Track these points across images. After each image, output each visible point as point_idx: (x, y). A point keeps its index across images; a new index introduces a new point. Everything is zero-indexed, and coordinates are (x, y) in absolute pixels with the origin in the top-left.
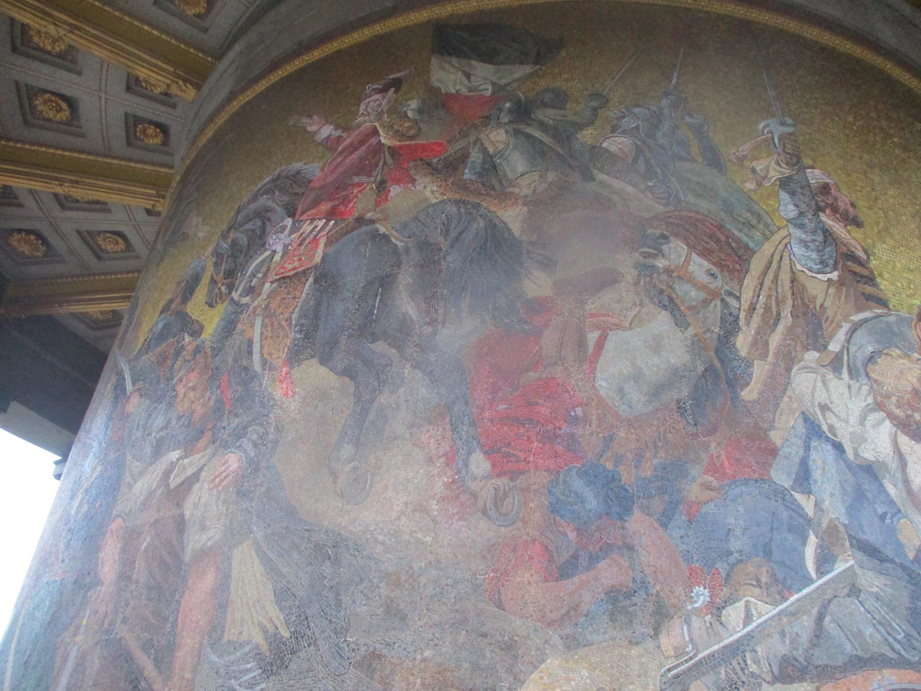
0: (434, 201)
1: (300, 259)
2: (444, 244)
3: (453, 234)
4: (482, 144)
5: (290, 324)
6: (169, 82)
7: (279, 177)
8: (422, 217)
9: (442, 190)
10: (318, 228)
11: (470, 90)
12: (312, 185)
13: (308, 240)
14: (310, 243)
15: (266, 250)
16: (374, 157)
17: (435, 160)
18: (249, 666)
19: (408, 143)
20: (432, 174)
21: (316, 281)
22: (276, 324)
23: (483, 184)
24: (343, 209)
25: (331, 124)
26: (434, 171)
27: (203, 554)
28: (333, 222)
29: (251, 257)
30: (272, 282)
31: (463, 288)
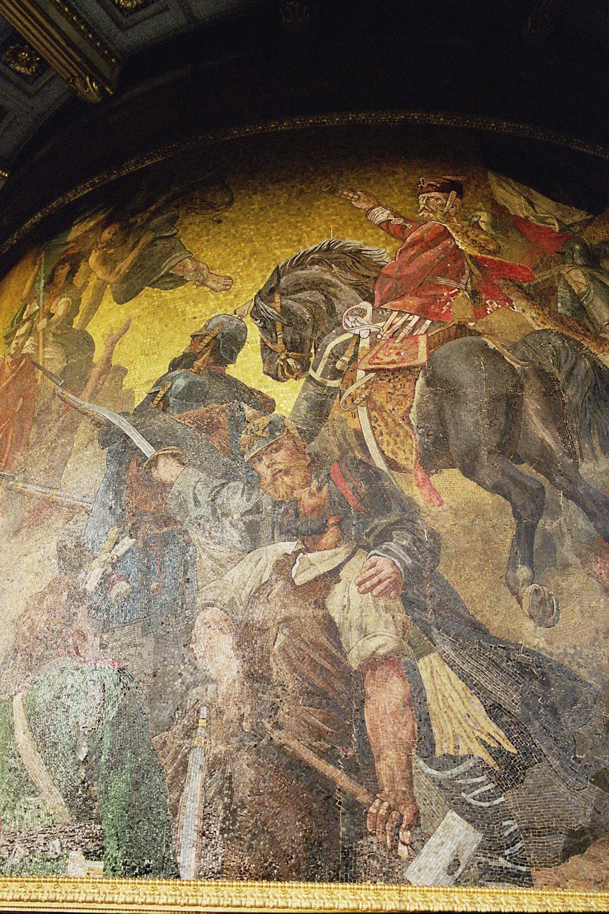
0: (537, 328)
1: (398, 354)
2: (561, 377)
3: (566, 368)
4: (567, 282)
5: (409, 423)
6: (76, 75)
7: (329, 249)
8: (530, 341)
9: (541, 318)
10: (412, 324)
11: (542, 220)
12: (383, 271)
13: (402, 335)
14: (404, 338)
15: (345, 332)
16: (455, 261)
17: (525, 285)
18: (479, 780)
19: (489, 257)
20: (528, 299)
21: (428, 383)
22: (389, 420)
23: (577, 321)
24: (437, 310)
25: (386, 207)
26: (528, 296)
27: (372, 663)
28: (428, 322)
29: (324, 335)
30: (367, 371)
31: (589, 425)
